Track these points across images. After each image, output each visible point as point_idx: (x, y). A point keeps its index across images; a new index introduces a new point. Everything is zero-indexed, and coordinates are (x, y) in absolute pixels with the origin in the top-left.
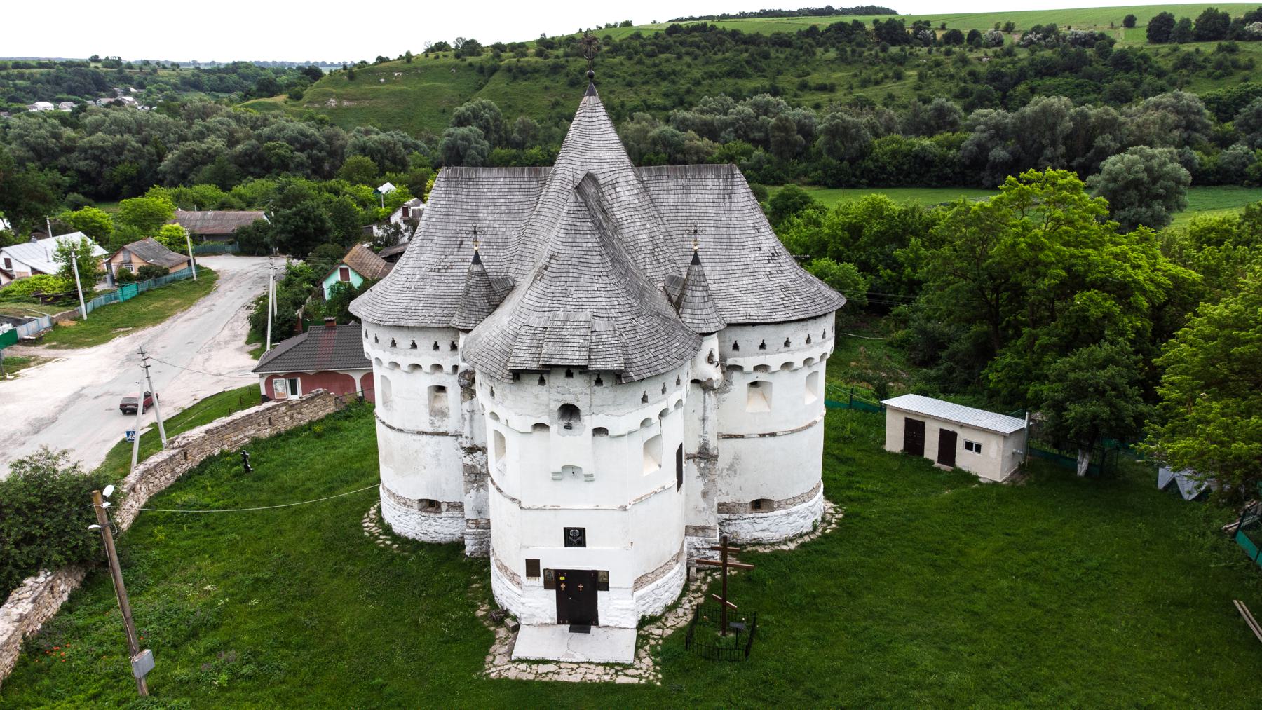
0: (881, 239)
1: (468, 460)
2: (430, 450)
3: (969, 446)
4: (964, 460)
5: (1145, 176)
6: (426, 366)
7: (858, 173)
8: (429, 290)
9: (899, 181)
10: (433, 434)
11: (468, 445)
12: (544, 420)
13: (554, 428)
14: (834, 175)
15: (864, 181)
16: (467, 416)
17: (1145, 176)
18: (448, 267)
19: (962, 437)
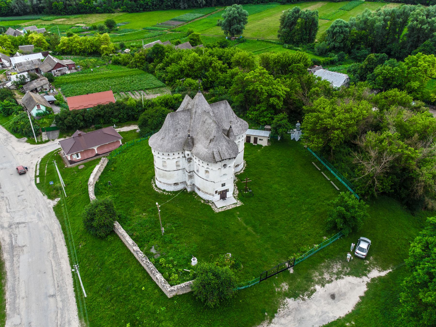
0: (201, 69)
1: (189, 174)
2: (176, 173)
3: (260, 140)
4: (259, 142)
5: (238, 15)
7: (138, 6)
8: (174, 142)
9: (153, 8)
12: (220, 167)
14: (130, 8)
15: (141, 9)
17: (238, 15)
18: (176, 136)
19: (259, 138)
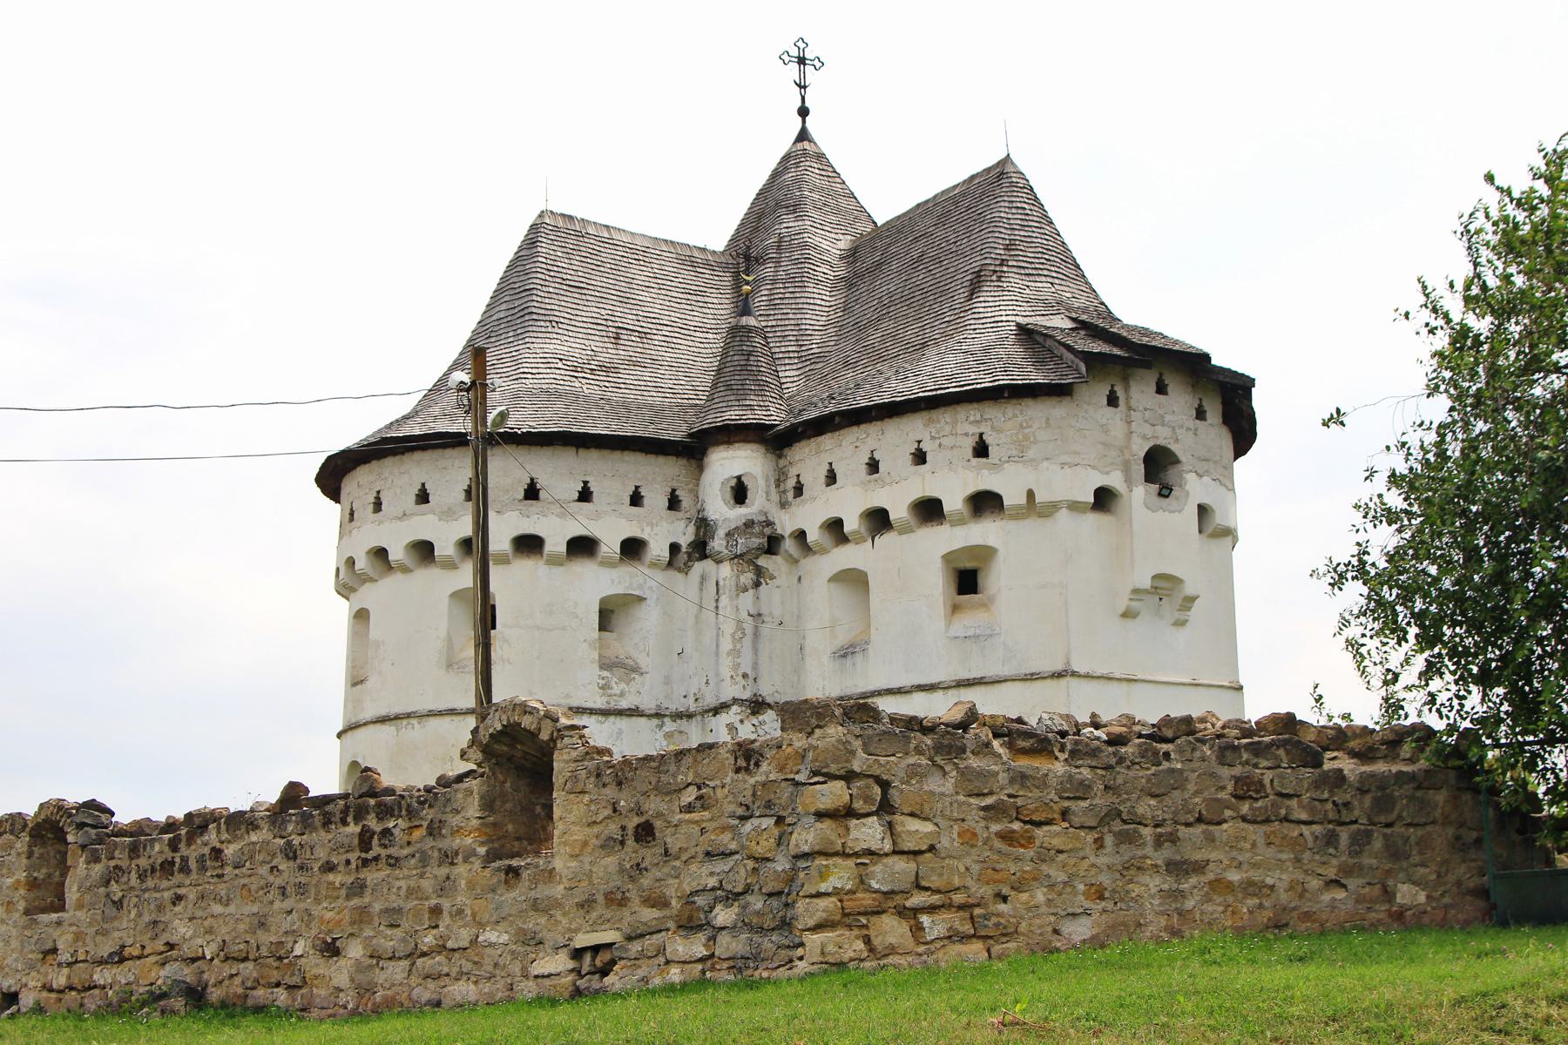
6: (610, 544)
10: (605, 713)
11: (746, 695)
12: (1115, 480)
13: (1138, 495)
16: (749, 625)
